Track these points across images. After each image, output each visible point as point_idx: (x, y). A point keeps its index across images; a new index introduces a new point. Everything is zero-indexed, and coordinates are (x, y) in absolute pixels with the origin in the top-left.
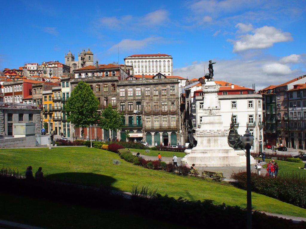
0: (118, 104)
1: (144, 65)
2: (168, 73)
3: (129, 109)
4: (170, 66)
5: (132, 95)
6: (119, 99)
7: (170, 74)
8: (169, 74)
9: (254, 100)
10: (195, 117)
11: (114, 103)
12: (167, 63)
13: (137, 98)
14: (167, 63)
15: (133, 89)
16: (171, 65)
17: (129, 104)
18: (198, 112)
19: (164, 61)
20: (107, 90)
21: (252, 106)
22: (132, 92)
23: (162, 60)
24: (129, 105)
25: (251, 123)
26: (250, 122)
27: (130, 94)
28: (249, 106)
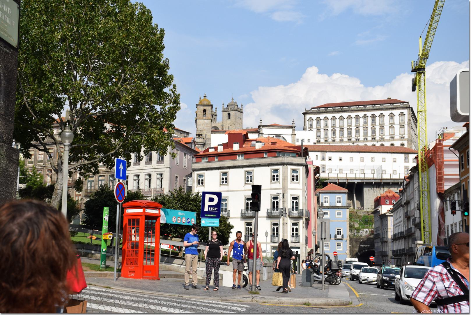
1: (345, 125)
2: (401, 142)
4: (406, 126)
7: (405, 143)
8: (402, 144)
9: (280, 167)
12: (397, 119)
14: (397, 119)
16: (406, 123)
19: (392, 115)
21: (277, 179)
23: (386, 113)
25: (295, 212)
26: (274, 207)
28: (274, 180)
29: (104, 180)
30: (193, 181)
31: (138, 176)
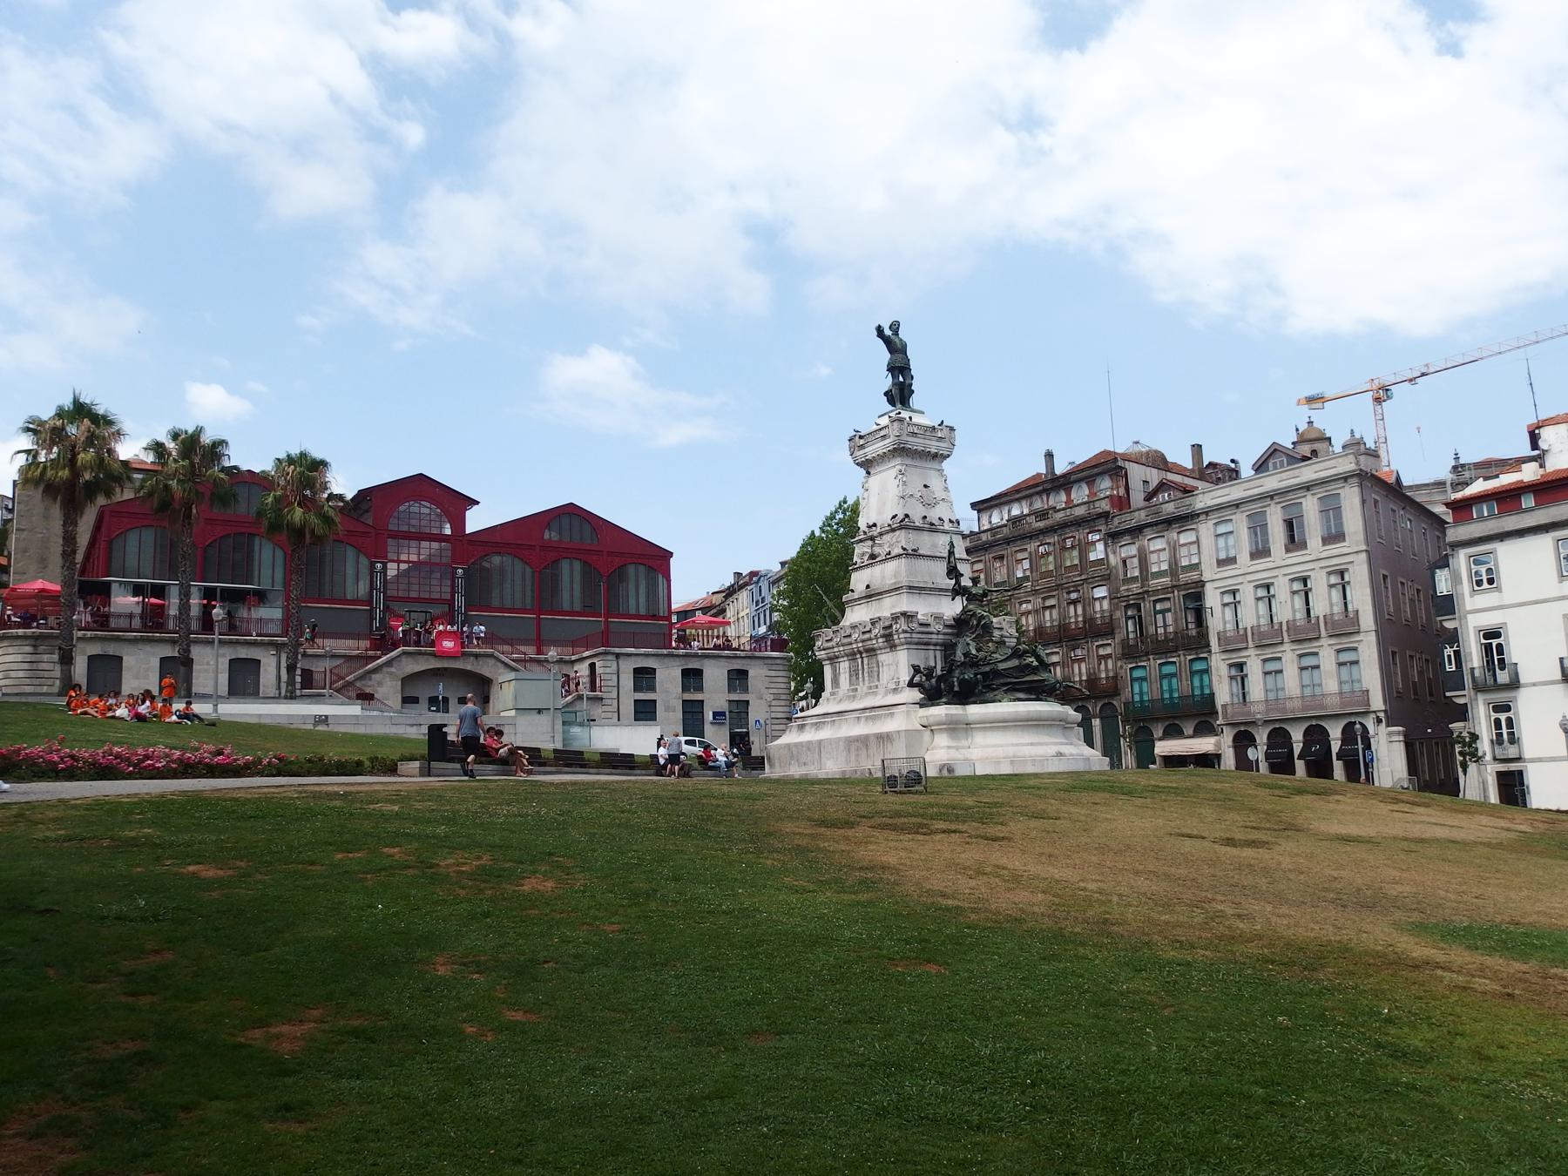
0: (1118, 614)
3: (1161, 631)
5: (1165, 567)
6: (1118, 591)
10: (1453, 637)
11: (1102, 611)
13: (1184, 578)
15: (1169, 543)
17: (1158, 607)
18: (1468, 608)
20: (1076, 562)
22: (1165, 556)
24: (1156, 612)
27: (1159, 563)
29: (1169, 610)
30: (1456, 579)
31: (1305, 580)
